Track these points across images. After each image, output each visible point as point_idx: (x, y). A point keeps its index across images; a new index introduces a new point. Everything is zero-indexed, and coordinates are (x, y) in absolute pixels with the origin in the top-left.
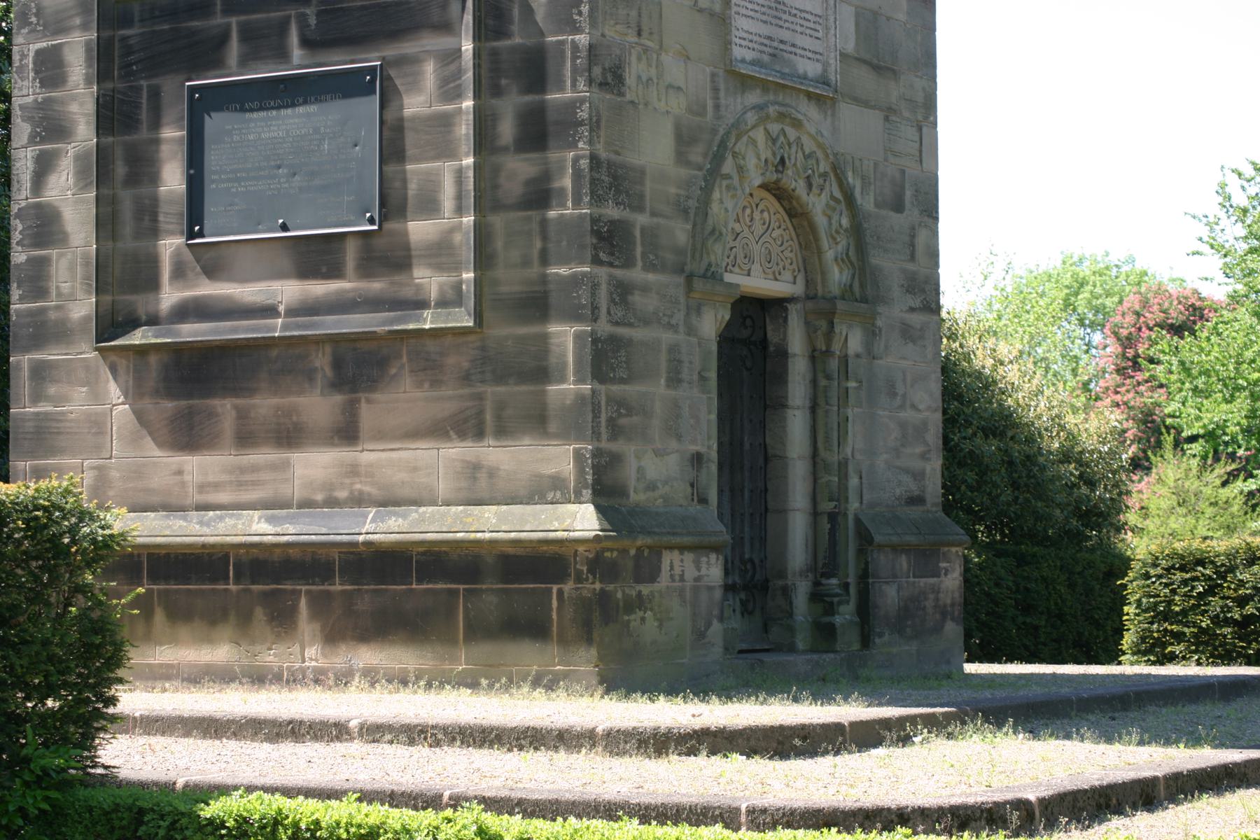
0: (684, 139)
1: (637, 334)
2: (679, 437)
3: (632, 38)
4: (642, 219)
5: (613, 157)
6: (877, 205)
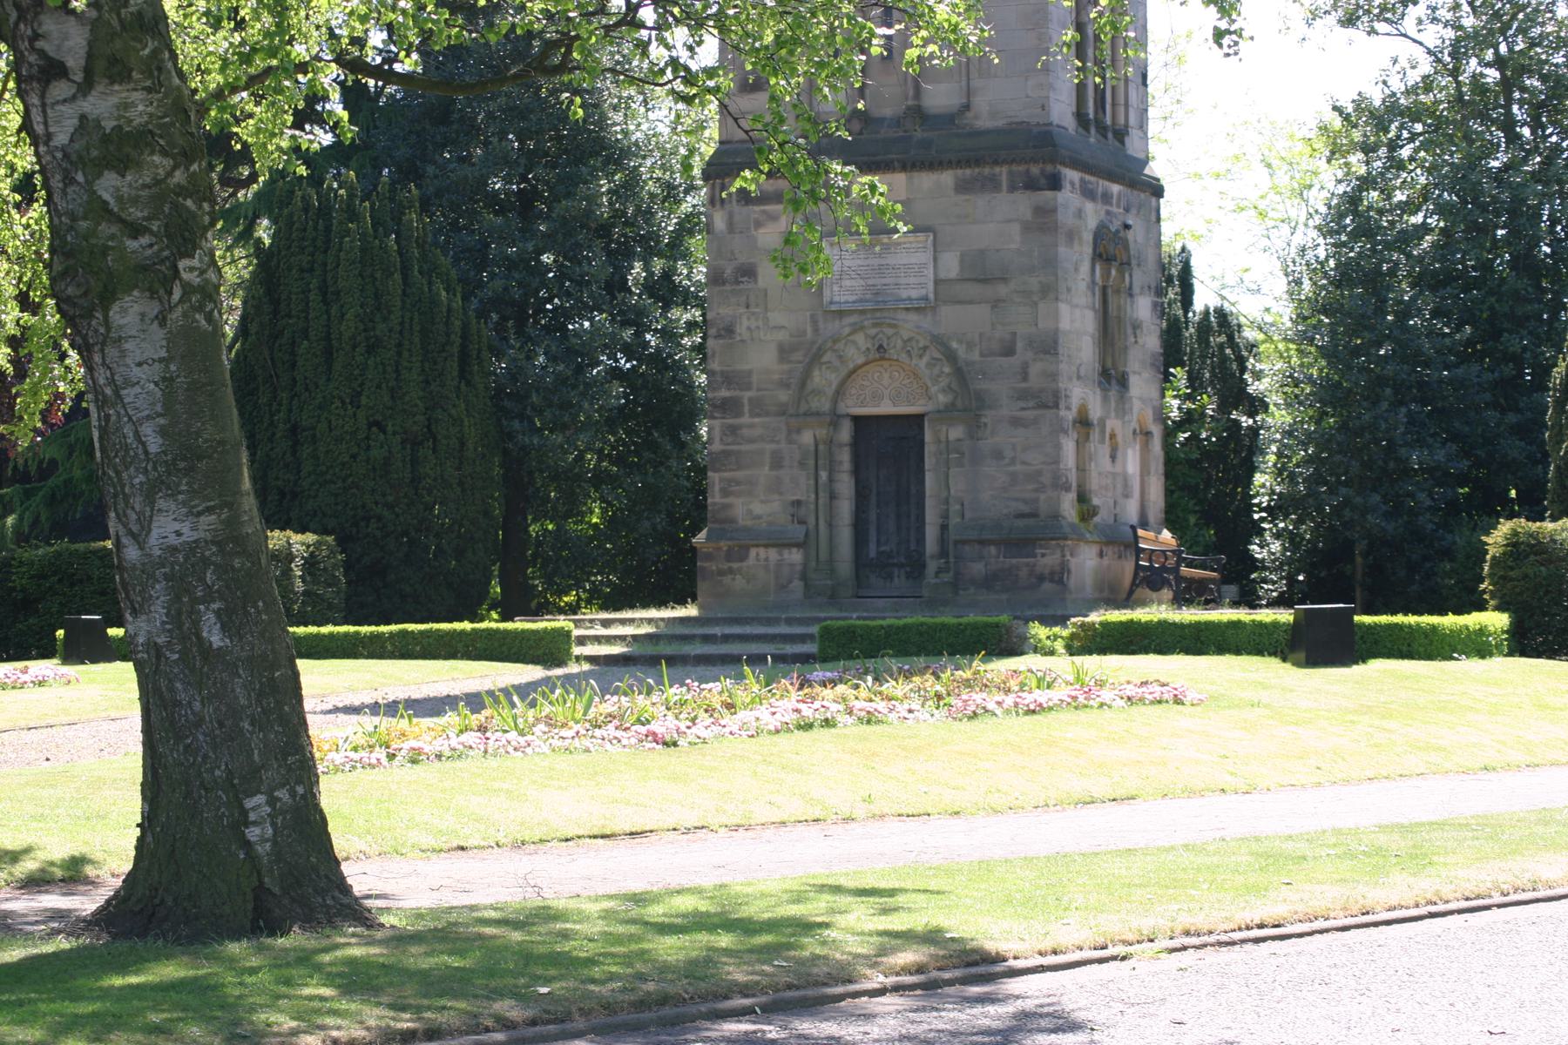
0: (784, 352)
1: (745, 447)
2: (781, 494)
3: (742, 310)
4: (748, 394)
6: (982, 355)
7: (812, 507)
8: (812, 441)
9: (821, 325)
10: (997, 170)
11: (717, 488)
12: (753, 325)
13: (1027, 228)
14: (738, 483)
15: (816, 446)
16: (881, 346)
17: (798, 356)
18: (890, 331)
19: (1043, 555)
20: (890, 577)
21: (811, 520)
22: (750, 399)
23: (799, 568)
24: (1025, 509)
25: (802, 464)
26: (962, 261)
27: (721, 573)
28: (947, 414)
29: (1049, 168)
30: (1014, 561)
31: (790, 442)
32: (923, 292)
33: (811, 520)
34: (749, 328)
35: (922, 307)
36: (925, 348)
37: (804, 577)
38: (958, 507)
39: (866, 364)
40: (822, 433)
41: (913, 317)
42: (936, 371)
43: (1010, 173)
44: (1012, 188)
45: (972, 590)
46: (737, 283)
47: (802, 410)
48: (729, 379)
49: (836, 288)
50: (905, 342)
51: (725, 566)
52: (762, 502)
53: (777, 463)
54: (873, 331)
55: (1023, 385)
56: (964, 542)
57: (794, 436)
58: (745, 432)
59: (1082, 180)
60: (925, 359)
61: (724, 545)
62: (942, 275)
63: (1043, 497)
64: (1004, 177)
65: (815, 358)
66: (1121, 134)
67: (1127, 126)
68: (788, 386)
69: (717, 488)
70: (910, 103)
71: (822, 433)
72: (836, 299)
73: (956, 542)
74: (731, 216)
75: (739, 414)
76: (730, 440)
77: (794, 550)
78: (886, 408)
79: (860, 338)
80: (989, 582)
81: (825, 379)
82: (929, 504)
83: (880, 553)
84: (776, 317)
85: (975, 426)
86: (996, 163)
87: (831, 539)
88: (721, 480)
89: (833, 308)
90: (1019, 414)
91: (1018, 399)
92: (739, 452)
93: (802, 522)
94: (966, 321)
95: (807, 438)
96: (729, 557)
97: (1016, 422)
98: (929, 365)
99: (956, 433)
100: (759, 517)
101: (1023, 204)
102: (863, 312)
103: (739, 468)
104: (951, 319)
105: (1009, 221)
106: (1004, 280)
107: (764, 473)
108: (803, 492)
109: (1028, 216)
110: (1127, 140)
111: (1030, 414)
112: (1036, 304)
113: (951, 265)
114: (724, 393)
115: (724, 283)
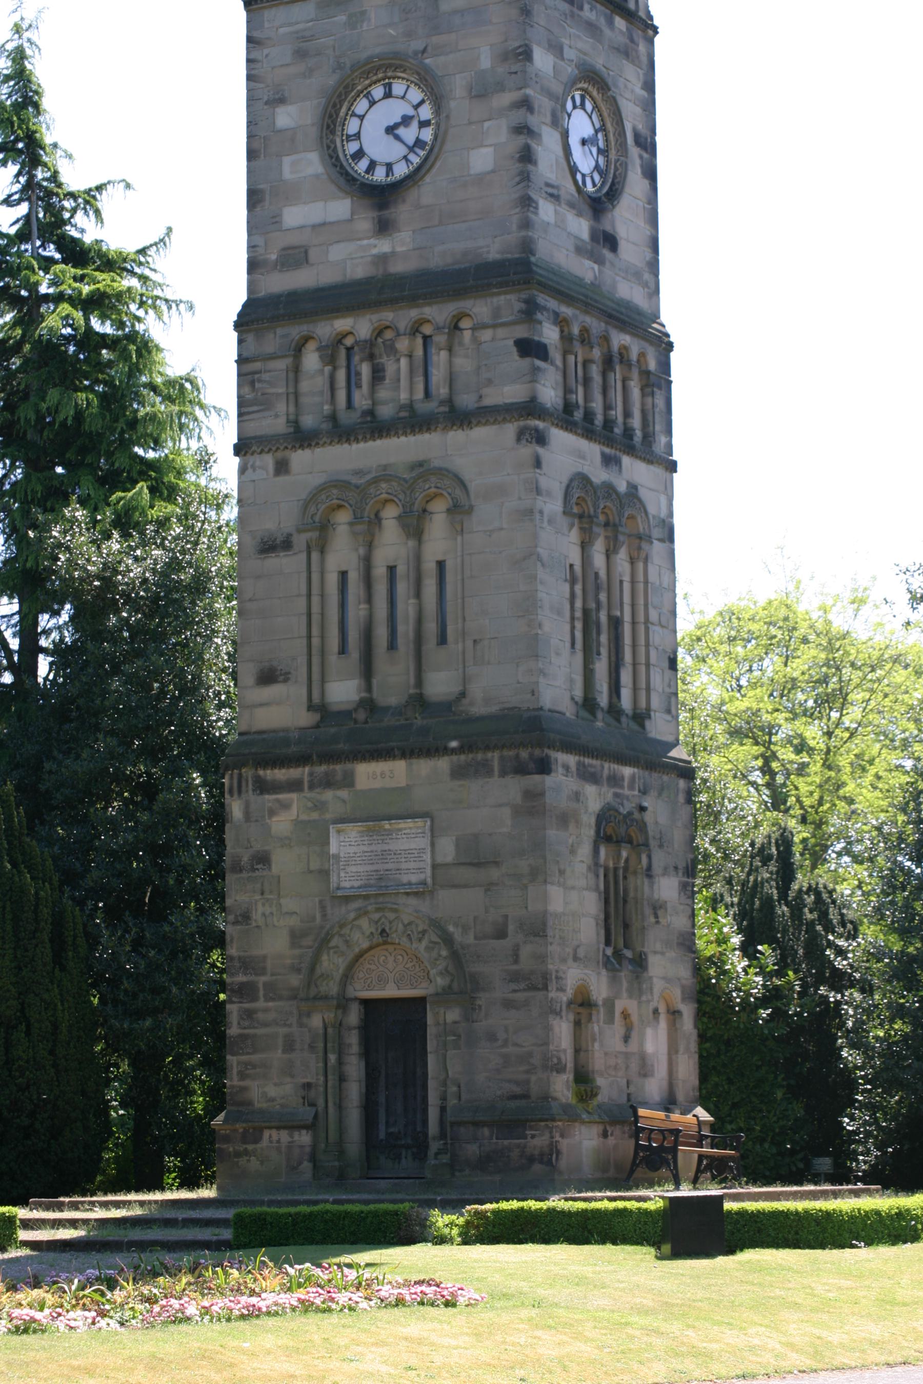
0: (296, 937)
1: (260, 1031)
2: (292, 1076)
3: (258, 897)
4: (263, 979)
5: (242, 954)
6: (476, 938)
7: (322, 1089)
8: (321, 1025)
9: (329, 911)
10: (490, 755)
11: (235, 1071)
12: (268, 910)
13: (517, 812)
14: (254, 1067)
15: (326, 1028)
16: (383, 931)
17: (308, 941)
18: (391, 916)
19: (533, 1137)
20: (398, 1158)
21: (321, 1102)
22: (265, 984)
23: (308, 1150)
24: (518, 1090)
25: (312, 1048)
26: (457, 846)
27: (238, 1154)
28: (445, 996)
29: (537, 752)
30: (506, 1142)
31: (301, 1025)
32: (422, 876)
33: (321, 1102)
34: (264, 915)
35: (420, 892)
36: (424, 932)
37: (313, 1158)
38: (455, 1089)
39: (371, 948)
40: (330, 1016)
41: (413, 901)
42: (434, 954)
43: (502, 758)
44: (503, 774)
45: (467, 1172)
46: (254, 870)
47: (312, 994)
48: (247, 964)
49: (342, 874)
50: (405, 926)
51: (241, 1148)
52: (275, 1085)
53: (289, 1046)
54: (376, 916)
55: (515, 967)
56: (460, 1124)
57: (305, 1020)
58: (260, 1016)
59: (579, 764)
60: (424, 943)
61: (240, 1127)
62: (439, 859)
63: (533, 1078)
64: (496, 765)
65: (324, 943)
66: (641, 717)
67: (648, 709)
68: (299, 971)
69: (235, 1071)
70: (412, 691)
71: (330, 1016)
72: (343, 884)
73: (453, 1124)
74: (247, 806)
75: (255, 999)
76: (247, 1023)
77: (304, 1132)
78: (391, 992)
79: (364, 923)
80: (484, 1163)
81: (332, 964)
82: (431, 1084)
83: (389, 1135)
84: (288, 904)
85: (470, 1010)
86: (487, 748)
87: (341, 1121)
88: (239, 1063)
89: (340, 893)
90: (511, 996)
91: (511, 981)
92: (255, 1036)
93: (312, 1104)
94: (459, 905)
95: (316, 1021)
96: (245, 1139)
97: (508, 1004)
98: (427, 949)
99: (453, 1015)
100: (273, 1100)
101: (511, 788)
102: (366, 897)
103: (255, 1052)
104: (448, 903)
105: (500, 806)
106: (496, 864)
107: (277, 1056)
108: (313, 1075)
109: (518, 799)
110: (647, 723)
111: (520, 996)
112: (525, 887)
113: (447, 849)
114: (241, 978)
115: (241, 871)
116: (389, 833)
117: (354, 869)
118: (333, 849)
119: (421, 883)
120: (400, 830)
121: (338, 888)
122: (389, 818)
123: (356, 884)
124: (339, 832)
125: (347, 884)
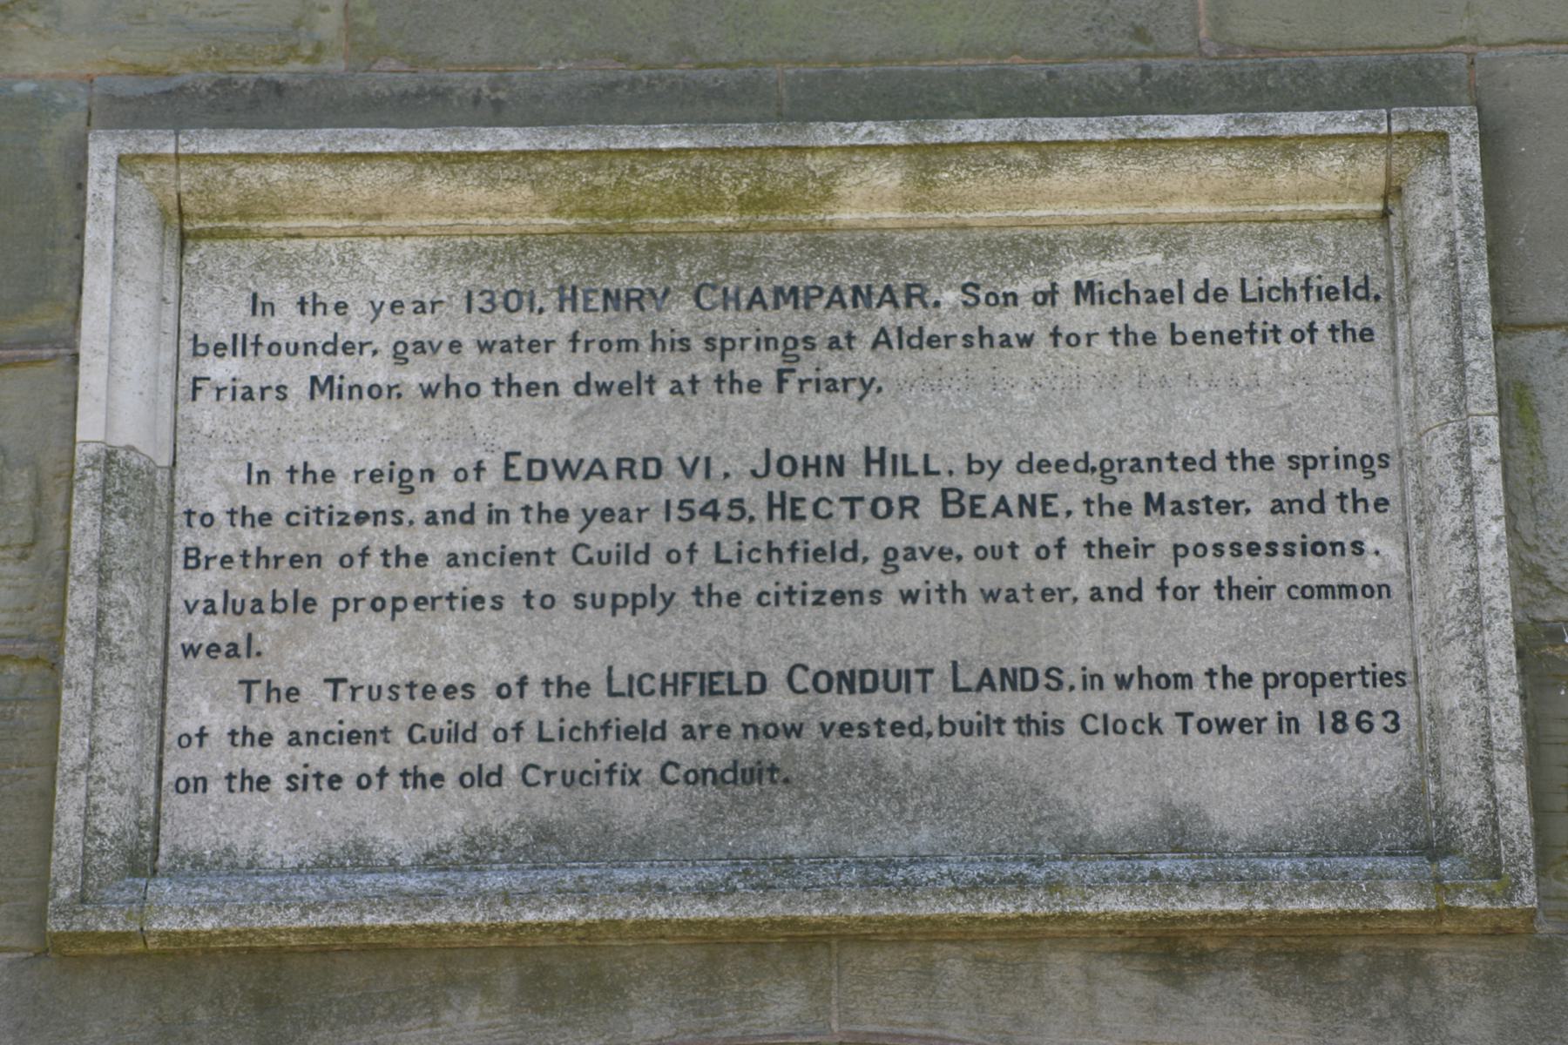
32: (1369, 768)
49: (204, 704)
72: (197, 825)
89: (175, 912)
116: (885, 279)
117: (375, 650)
118: (117, 398)
119: (1341, 840)
120: (1036, 248)
121: (141, 862)
122: (910, 96)
123: (399, 825)
124: (183, 232)
125: (276, 829)
